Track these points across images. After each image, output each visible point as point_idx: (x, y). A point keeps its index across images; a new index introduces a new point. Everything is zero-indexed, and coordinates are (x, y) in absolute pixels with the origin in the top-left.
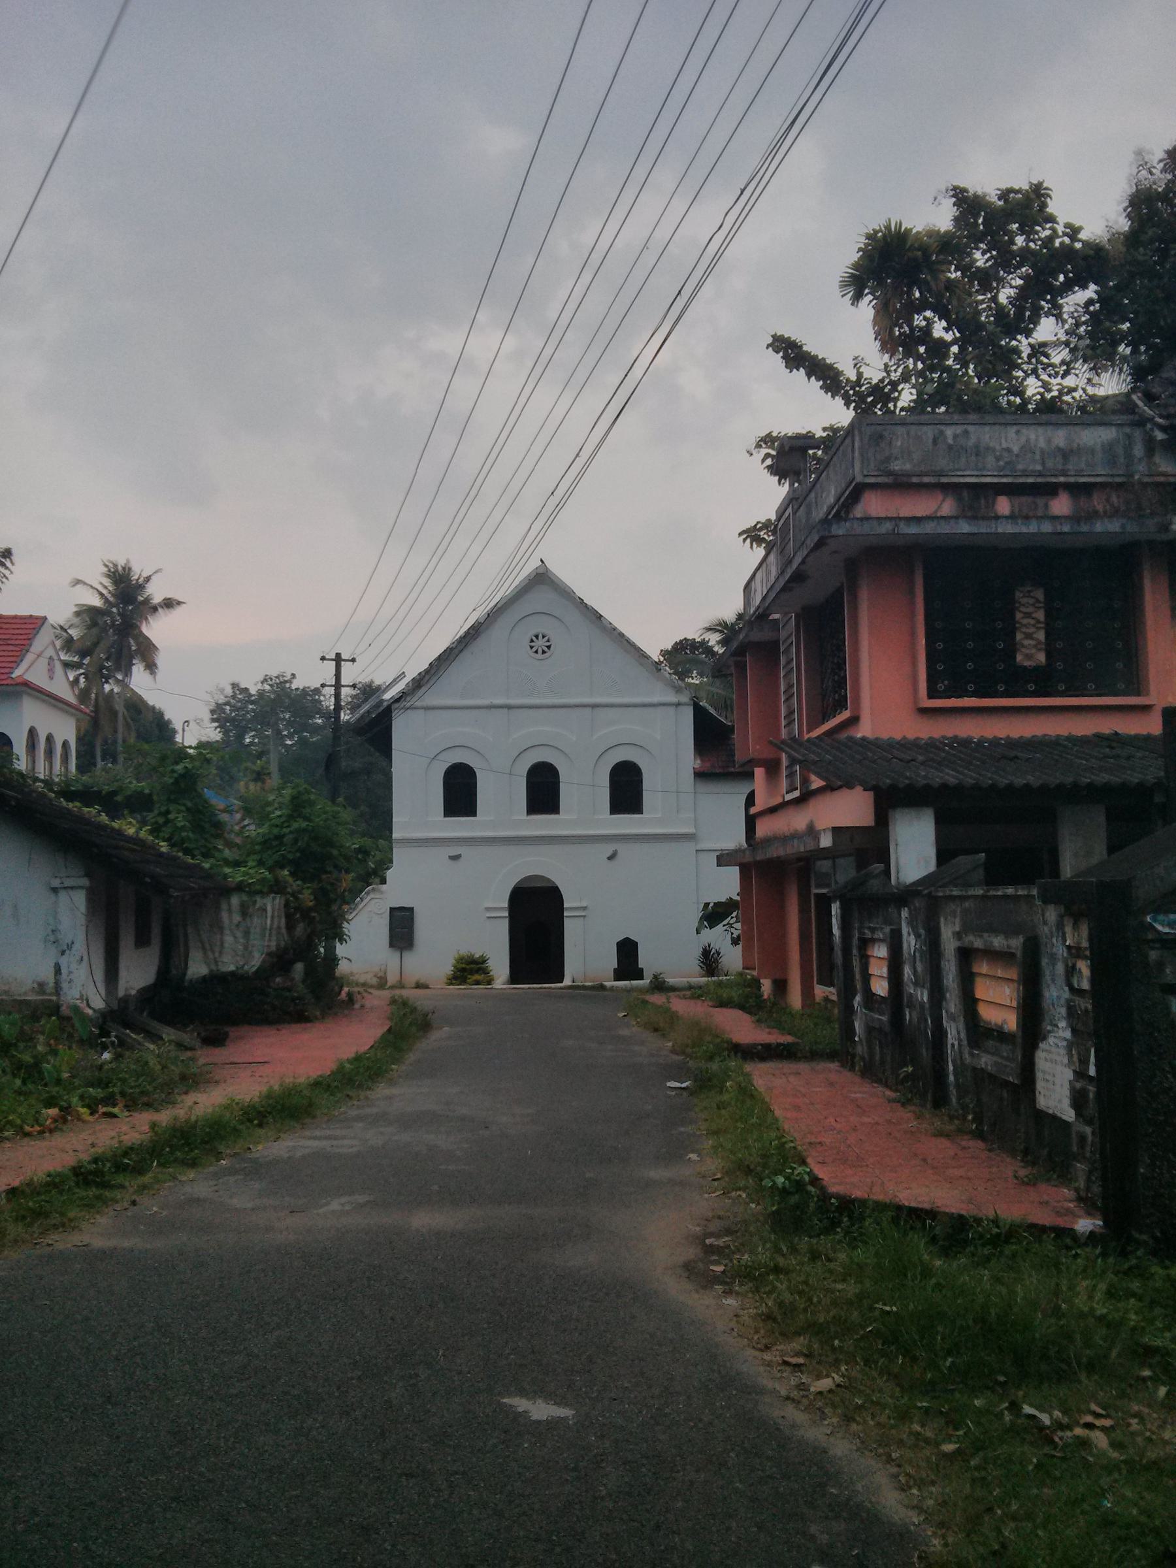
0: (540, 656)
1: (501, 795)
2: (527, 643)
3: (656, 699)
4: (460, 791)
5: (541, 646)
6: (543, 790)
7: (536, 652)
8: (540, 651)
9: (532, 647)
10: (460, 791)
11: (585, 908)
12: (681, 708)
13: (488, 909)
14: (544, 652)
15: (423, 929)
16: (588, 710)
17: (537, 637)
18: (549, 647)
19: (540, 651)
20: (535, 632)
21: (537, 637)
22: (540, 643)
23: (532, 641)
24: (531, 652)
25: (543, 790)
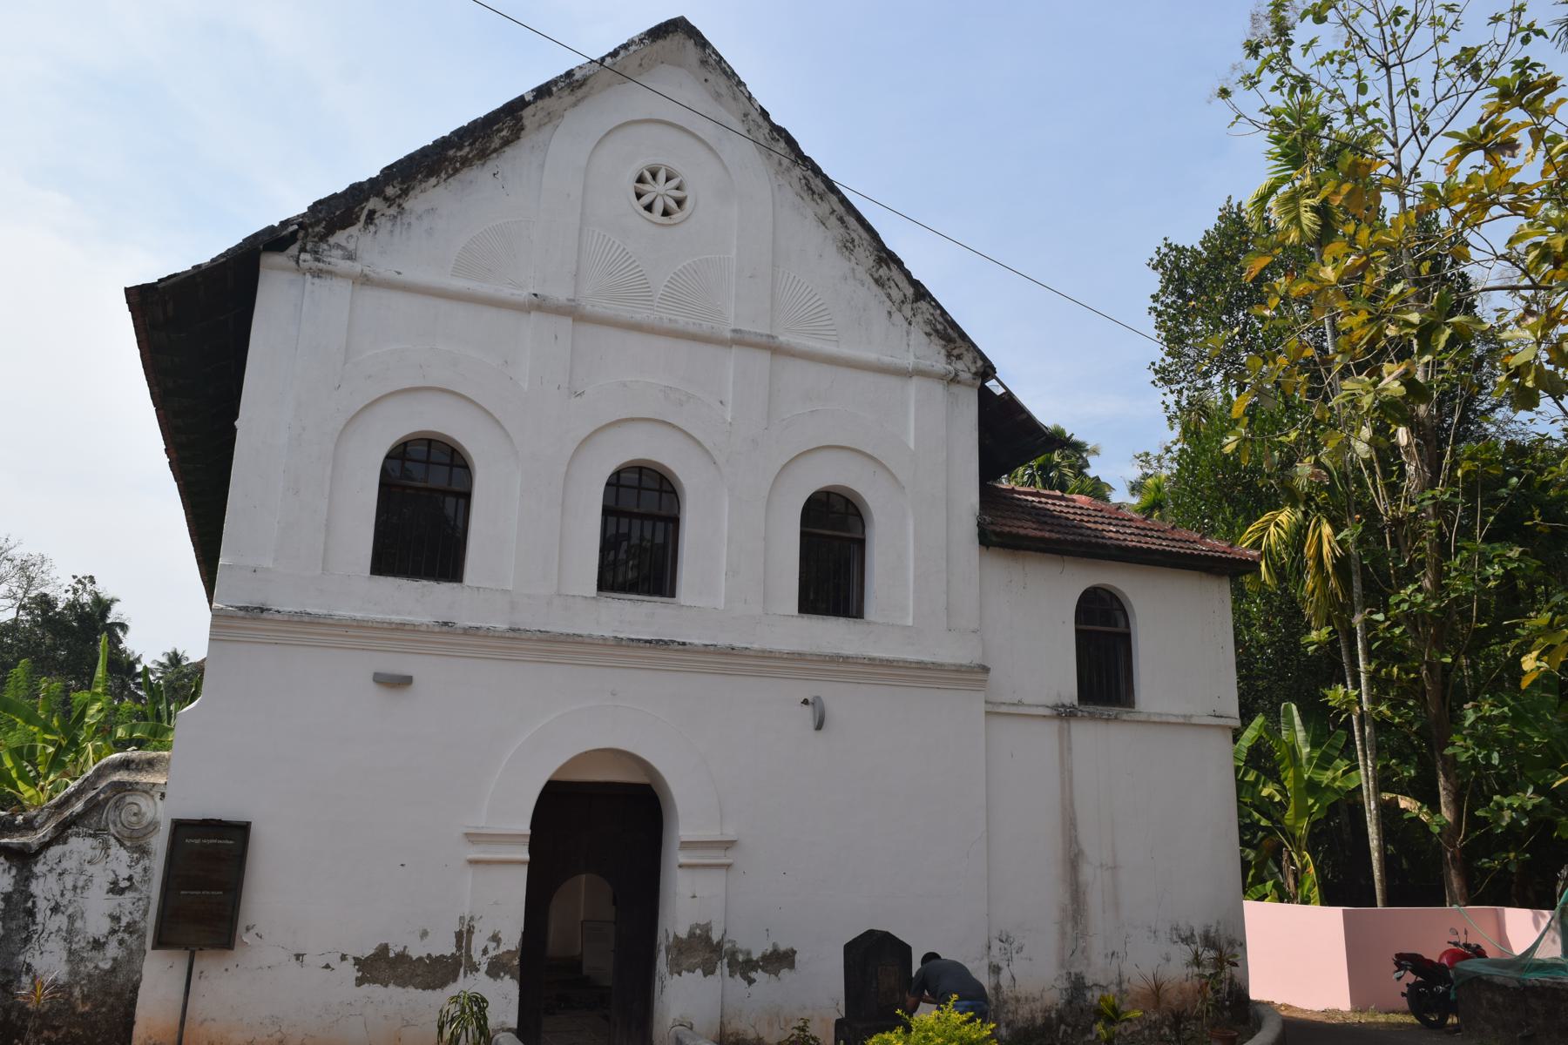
0: (656, 215)
1: (531, 535)
2: (630, 186)
3: (909, 361)
4: (422, 514)
5: (661, 198)
6: (640, 535)
7: (649, 208)
8: (658, 207)
9: (639, 196)
10: (422, 514)
11: (728, 845)
12: (955, 388)
13: (473, 838)
14: (666, 213)
15: (272, 893)
16: (763, 358)
17: (654, 176)
18: (680, 203)
19: (658, 207)
20: (652, 161)
21: (654, 176)
22: (659, 191)
23: (641, 180)
24: (638, 206)
25: (640, 535)
